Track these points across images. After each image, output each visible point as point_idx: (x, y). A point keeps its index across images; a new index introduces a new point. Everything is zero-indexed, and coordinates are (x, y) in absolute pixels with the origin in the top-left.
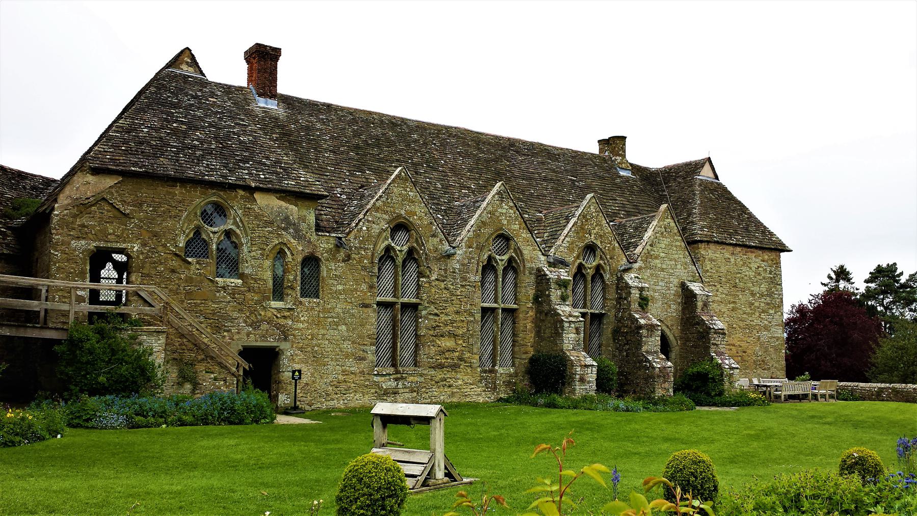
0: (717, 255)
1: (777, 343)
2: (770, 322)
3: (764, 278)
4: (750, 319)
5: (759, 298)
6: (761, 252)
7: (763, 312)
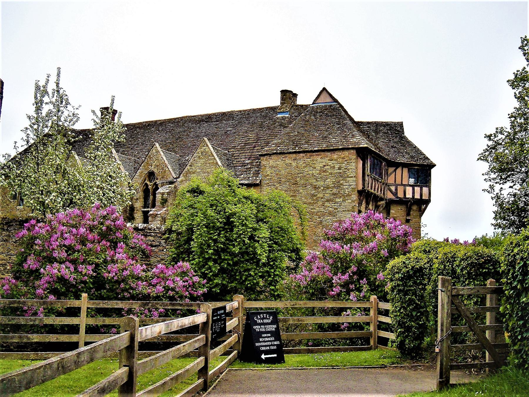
0: (278, 163)
3: (331, 174)
4: (311, 207)
5: (323, 190)
7: (328, 201)
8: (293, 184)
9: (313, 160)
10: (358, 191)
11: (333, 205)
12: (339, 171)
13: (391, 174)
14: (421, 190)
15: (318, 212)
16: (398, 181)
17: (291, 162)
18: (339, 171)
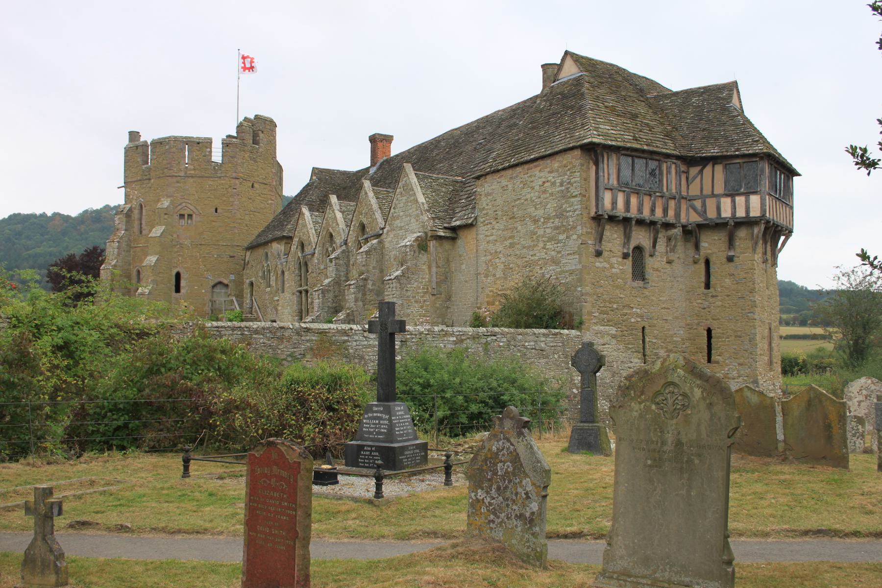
0: (493, 187)
1: (569, 279)
2: (559, 252)
3: (552, 195)
4: (531, 253)
5: (543, 223)
6: (549, 161)
7: (550, 239)
8: (510, 219)
9: (531, 176)
10: (593, 218)
11: (556, 245)
12: (560, 188)
13: (695, 178)
14: (747, 202)
15: (539, 260)
16: (707, 190)
17: (507, 183)
18: (560, 188)
